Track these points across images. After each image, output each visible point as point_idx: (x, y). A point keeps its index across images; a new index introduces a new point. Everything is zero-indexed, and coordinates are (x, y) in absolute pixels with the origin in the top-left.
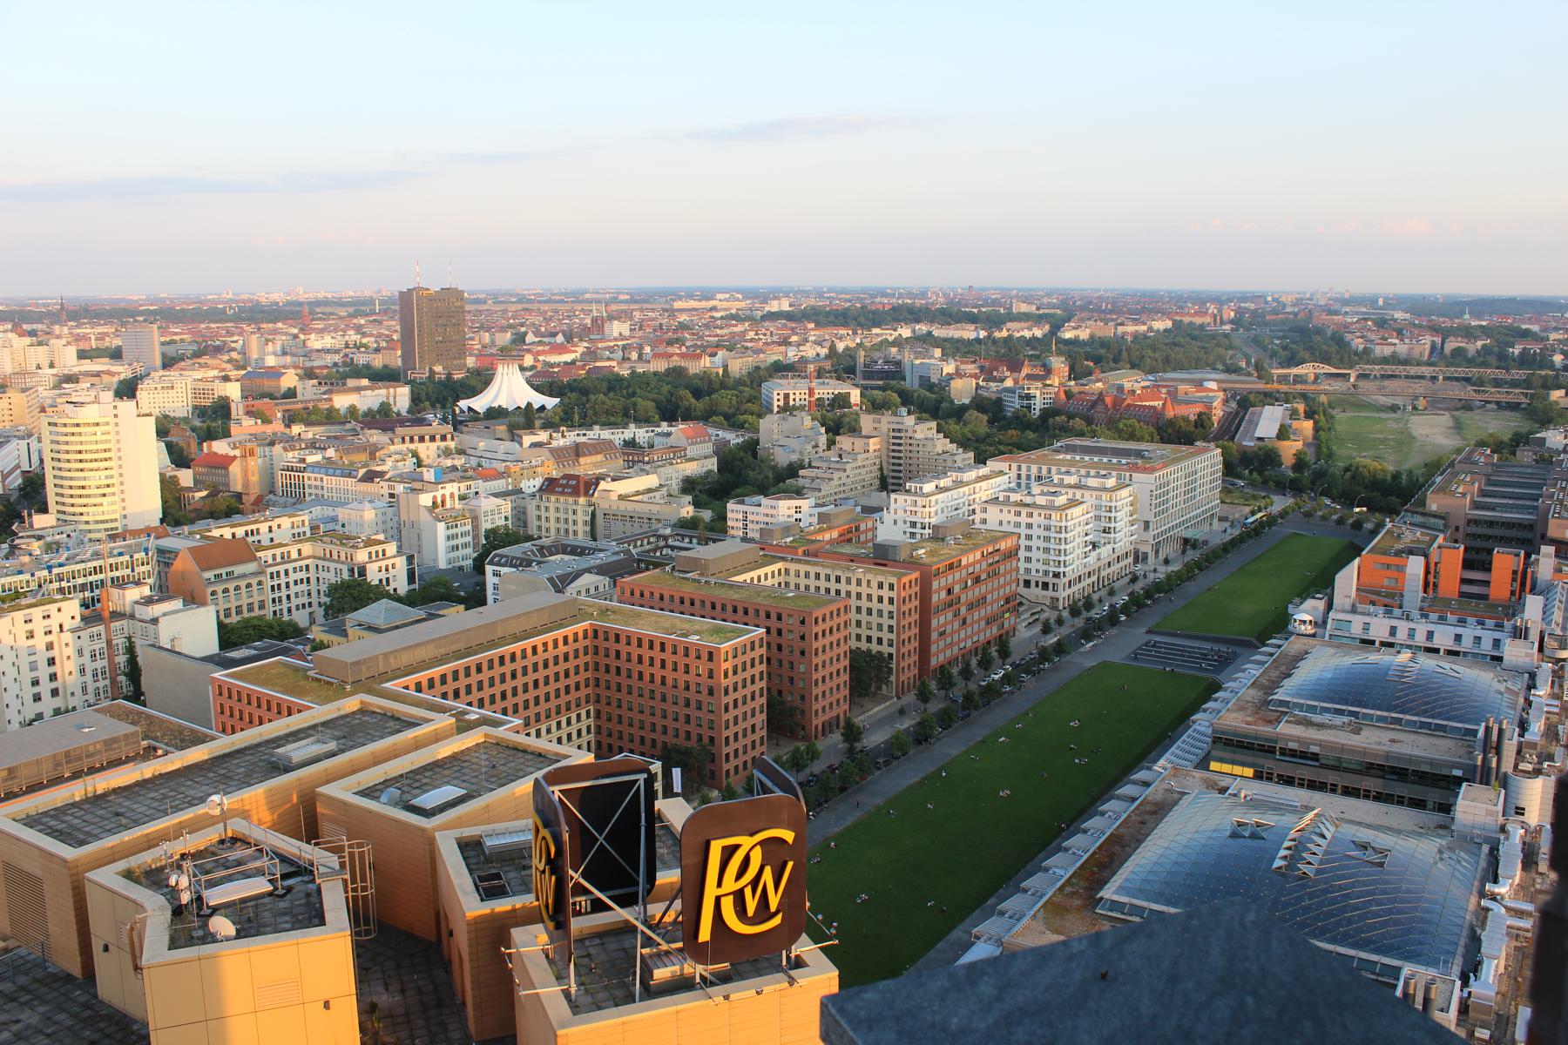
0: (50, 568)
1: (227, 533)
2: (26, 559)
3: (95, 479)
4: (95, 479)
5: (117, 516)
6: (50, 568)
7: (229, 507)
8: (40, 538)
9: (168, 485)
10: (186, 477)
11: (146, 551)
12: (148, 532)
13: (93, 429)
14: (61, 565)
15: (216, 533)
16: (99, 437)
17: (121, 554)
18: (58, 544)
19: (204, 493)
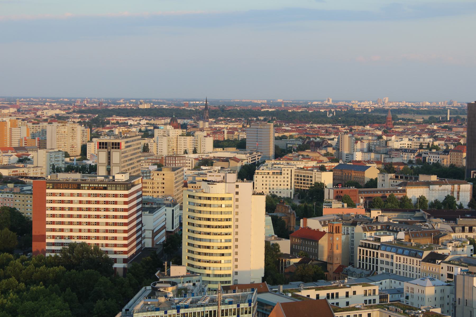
0: (178, 309)
1: (312, 294)
2: (162, 299)
3: (218, 241)
4: (218, 241)
5: (230, 272)
6: (178, 309)
7: (317, 273)
8: (173, 284)
9: (271, 251)
10: (285, 246)
11: (250, 302)
12: (252, 286)
13: (220, 202)
14: (186, 307)
15: (304, 293)
16: (223, 209)
17: (230, 303)
18: (186, 289)
19: (297, 260)
